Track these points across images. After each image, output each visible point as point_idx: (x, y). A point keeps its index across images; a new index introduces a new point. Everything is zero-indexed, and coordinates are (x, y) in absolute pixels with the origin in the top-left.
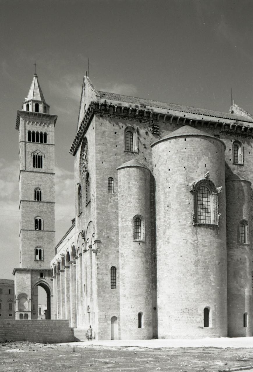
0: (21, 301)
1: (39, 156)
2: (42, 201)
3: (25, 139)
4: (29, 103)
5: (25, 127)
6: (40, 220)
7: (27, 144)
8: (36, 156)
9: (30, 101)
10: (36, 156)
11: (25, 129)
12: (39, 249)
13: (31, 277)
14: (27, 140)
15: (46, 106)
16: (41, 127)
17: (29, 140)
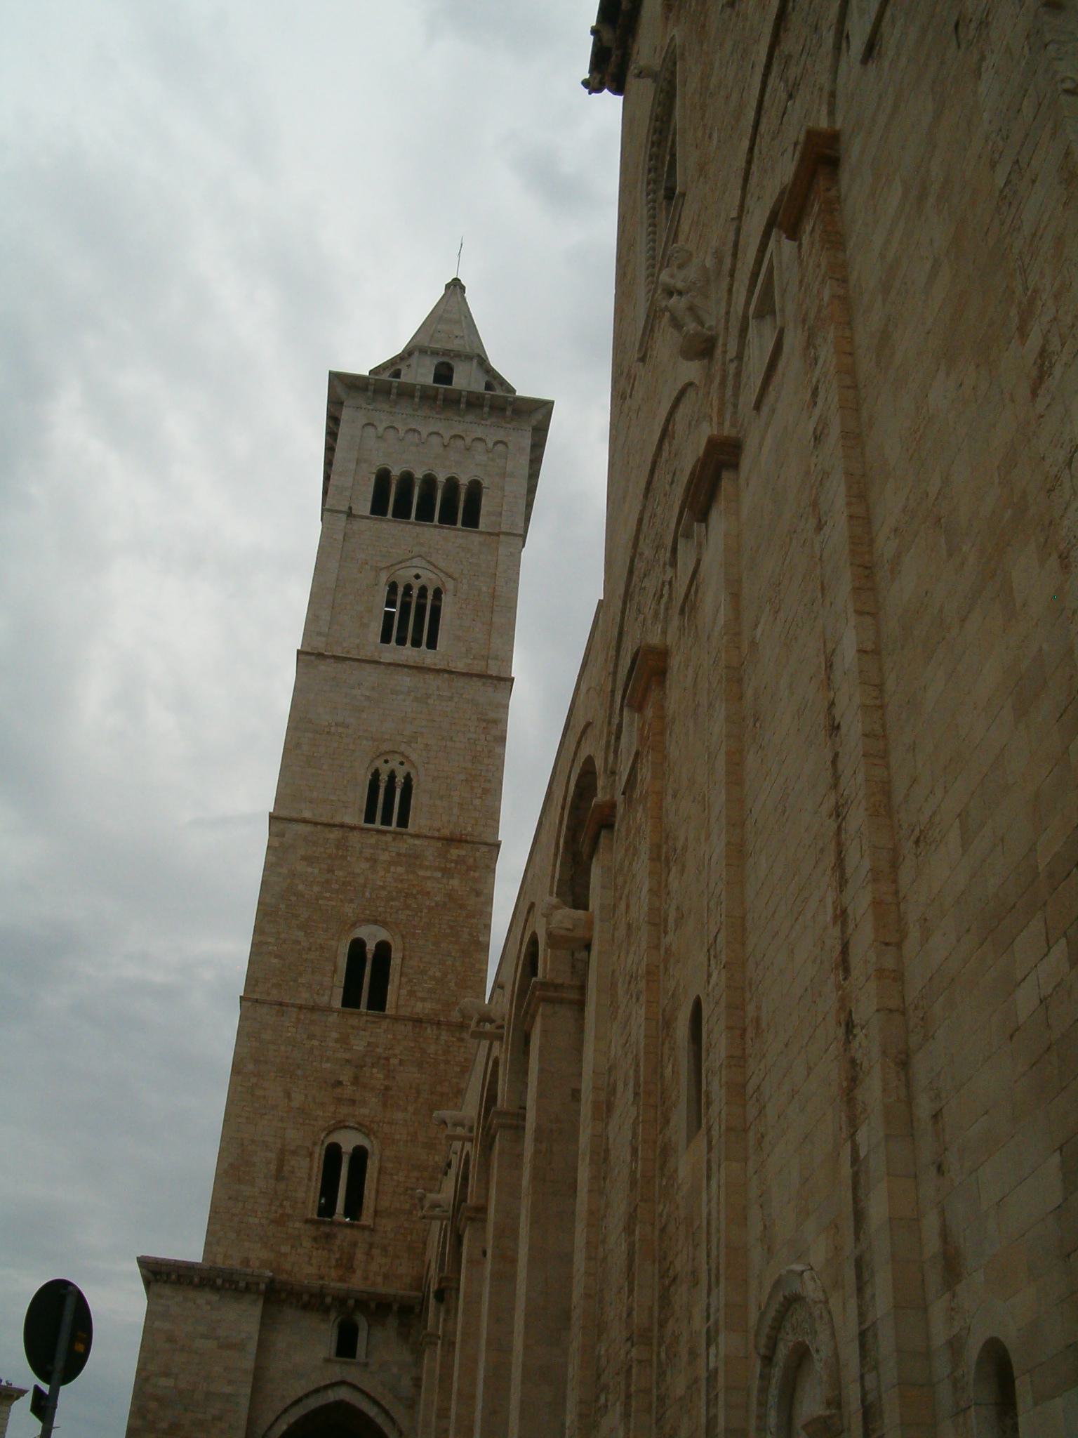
2: (411, 828)
8: (408, 588)
14: (364, 507)
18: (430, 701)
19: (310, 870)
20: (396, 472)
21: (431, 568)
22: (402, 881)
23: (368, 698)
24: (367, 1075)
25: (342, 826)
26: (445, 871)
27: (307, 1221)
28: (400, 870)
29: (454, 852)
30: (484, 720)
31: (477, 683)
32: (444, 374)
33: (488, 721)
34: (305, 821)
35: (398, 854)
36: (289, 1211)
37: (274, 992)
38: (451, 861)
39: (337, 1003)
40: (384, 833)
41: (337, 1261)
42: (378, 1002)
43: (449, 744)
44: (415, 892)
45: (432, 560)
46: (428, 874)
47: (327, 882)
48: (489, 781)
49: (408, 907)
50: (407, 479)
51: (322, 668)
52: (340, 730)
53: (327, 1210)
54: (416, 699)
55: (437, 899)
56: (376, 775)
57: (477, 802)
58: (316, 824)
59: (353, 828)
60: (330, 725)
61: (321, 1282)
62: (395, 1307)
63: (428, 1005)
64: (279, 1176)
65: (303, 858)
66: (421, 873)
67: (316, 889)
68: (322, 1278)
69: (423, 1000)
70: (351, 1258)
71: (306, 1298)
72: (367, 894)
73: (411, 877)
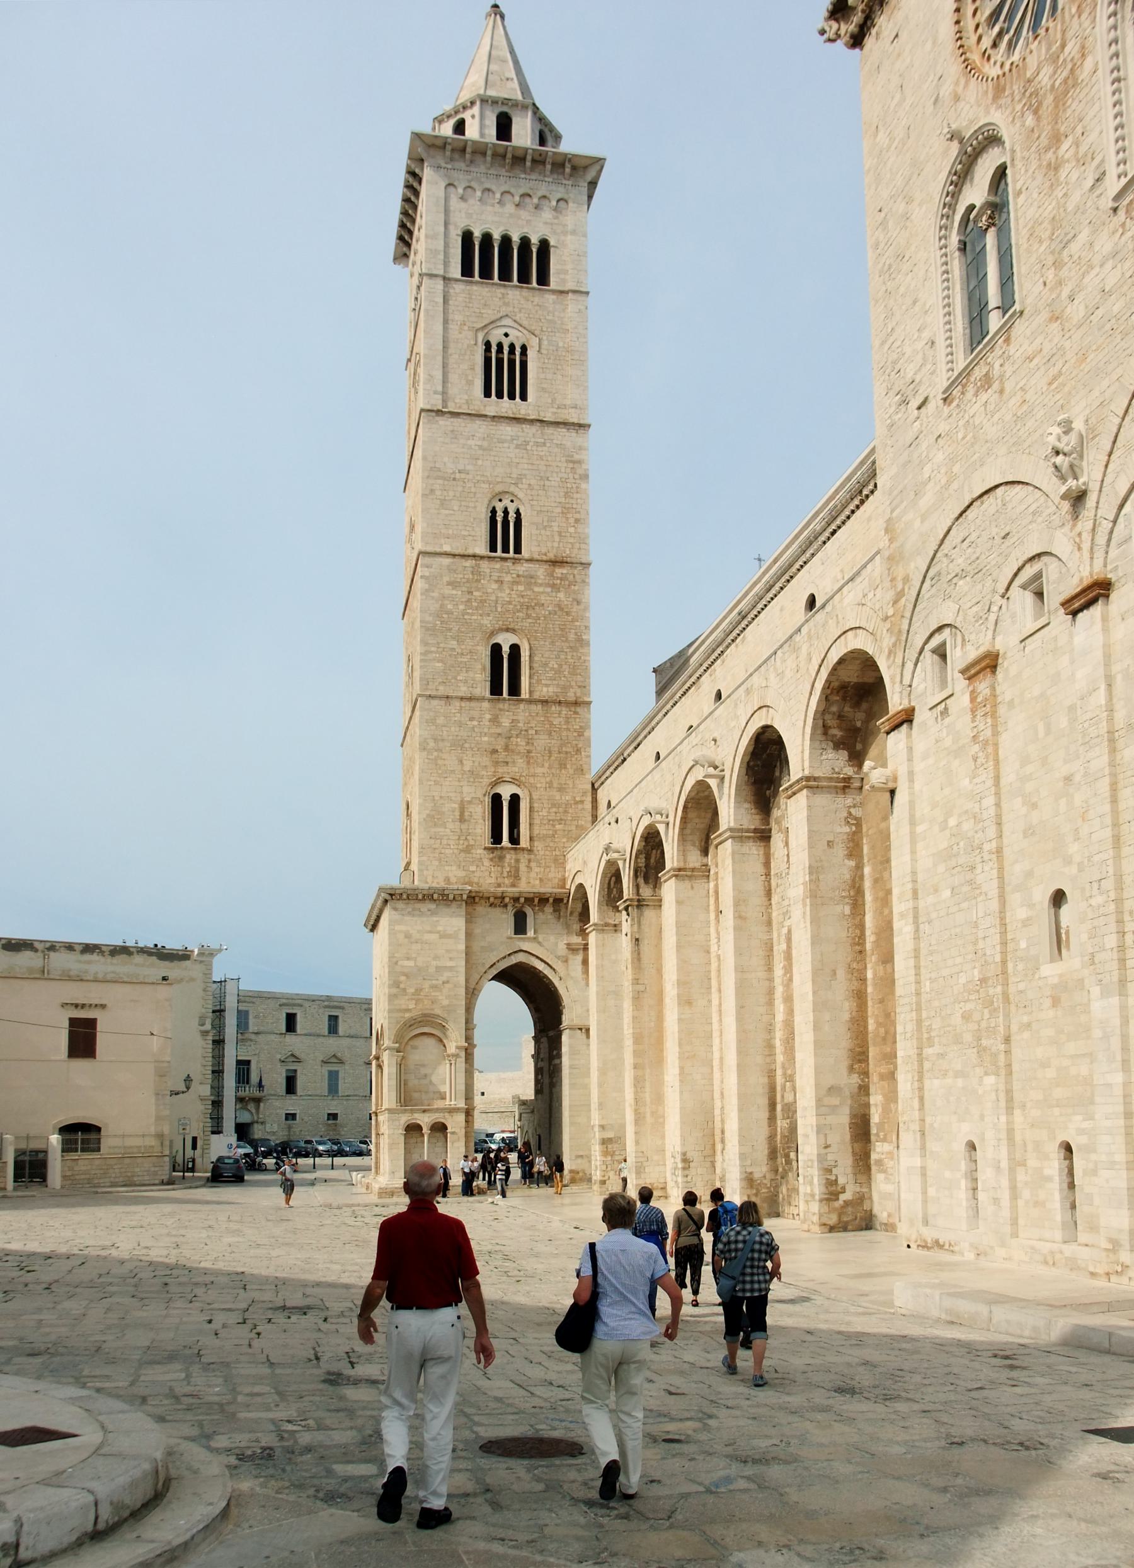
0: (415, 1057)
1: (512, 347)
2: (525, 552)
3: (446, 264)
4: (466, 115)
5: (447, 211)
6: (515, 649)
7: (459, 288)
8: (500, 346)
9: (473, 103)
10: (500, 346)
11: (446, 224)
12: (506, 792)
13: (469, 935)
14: (456, 271)
15: (546, 130)
16: (524, 214)
17: (467, 271)
18: (529, 447)
19: (454, 592)
20: (477, 234)
21: (516, 325)
23: (480, 447)
25: (474, 556)
26: (553, 586)
27: (485, 848)
28: (521, 588)
29: (559, 571)
30: (571, 462)
31: (562, 431)
32: (504, 127)
33: (574, 462)
34: (447, 554)
35: (518, 576)
36: (472, 842)
37: (441, 688)
39: (487, 694)
40: (505, 559)
42: (515, 690)
43: (547, 483)
45: (517, 318)
46: (541, 589)
47: (469, 600)
49: (528, 616)
50: (487, 238)
51: (441, 423)
52: (463, 476)
53: (496, 837)
54: (517, 447)
56: (494, 512)
57: (572, 530)
58: (454, 555)
59: (482, 557)
60: (454, 473)
62: (551, 900)
63: (551, 689)
64: (462, 819)
65: (449, 583)
66: (536, 589)
67: (462, 607)
69: (547, 686)
70: (517, 870)
71: (492, 900)
72: (499, 609)
73: (529, 593)
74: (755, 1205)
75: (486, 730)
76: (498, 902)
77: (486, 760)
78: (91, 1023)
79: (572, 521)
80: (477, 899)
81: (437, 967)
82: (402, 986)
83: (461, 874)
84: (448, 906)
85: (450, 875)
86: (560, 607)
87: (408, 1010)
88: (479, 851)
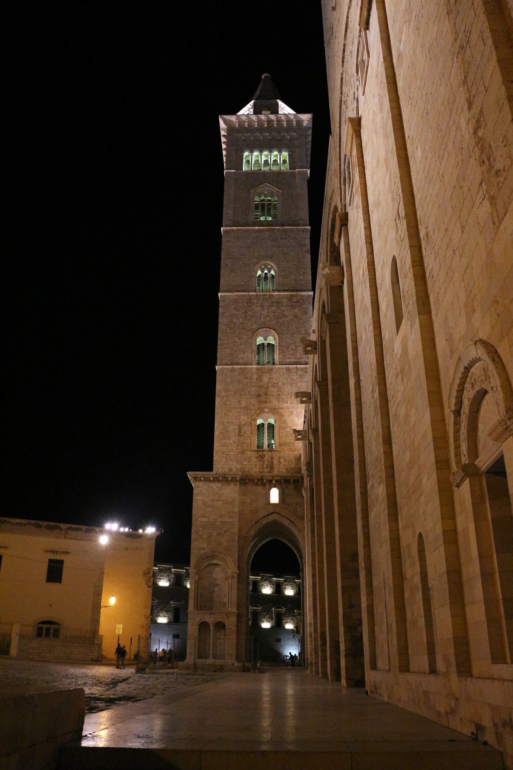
18: (278, 240)
22: (275, 312)
24: (270, 391)
27: (254, 451)
28: (274, 308)
33: (302, 245)
35: (272, 302)
36: (245, 448)
38: (294, 302)
41: (267, 465)
44: (281, 316)
46: (285, 308)
48: (305, 269)
55: (290, 318)
61: (261, 474)
62: (292, 481)
64: (240, 435)
66: (283, 308)
68: (262, 473)
69: (289, 358)
70: (272, 463)
71: (256, 481)
73: (278, 310)
74: (371, 670)
75: (254, 384)
76: (260, 482)
77: (254, 401)
78: (61, 562)
79: (301, 273)
80: (247, 481)
81: (221, 522)
82: (200, 533)
83: (239, 466)
84: (229, 485)
85: (232, 467)
86: (296, 316)
87: (204, 549)
88: (249, 453)
